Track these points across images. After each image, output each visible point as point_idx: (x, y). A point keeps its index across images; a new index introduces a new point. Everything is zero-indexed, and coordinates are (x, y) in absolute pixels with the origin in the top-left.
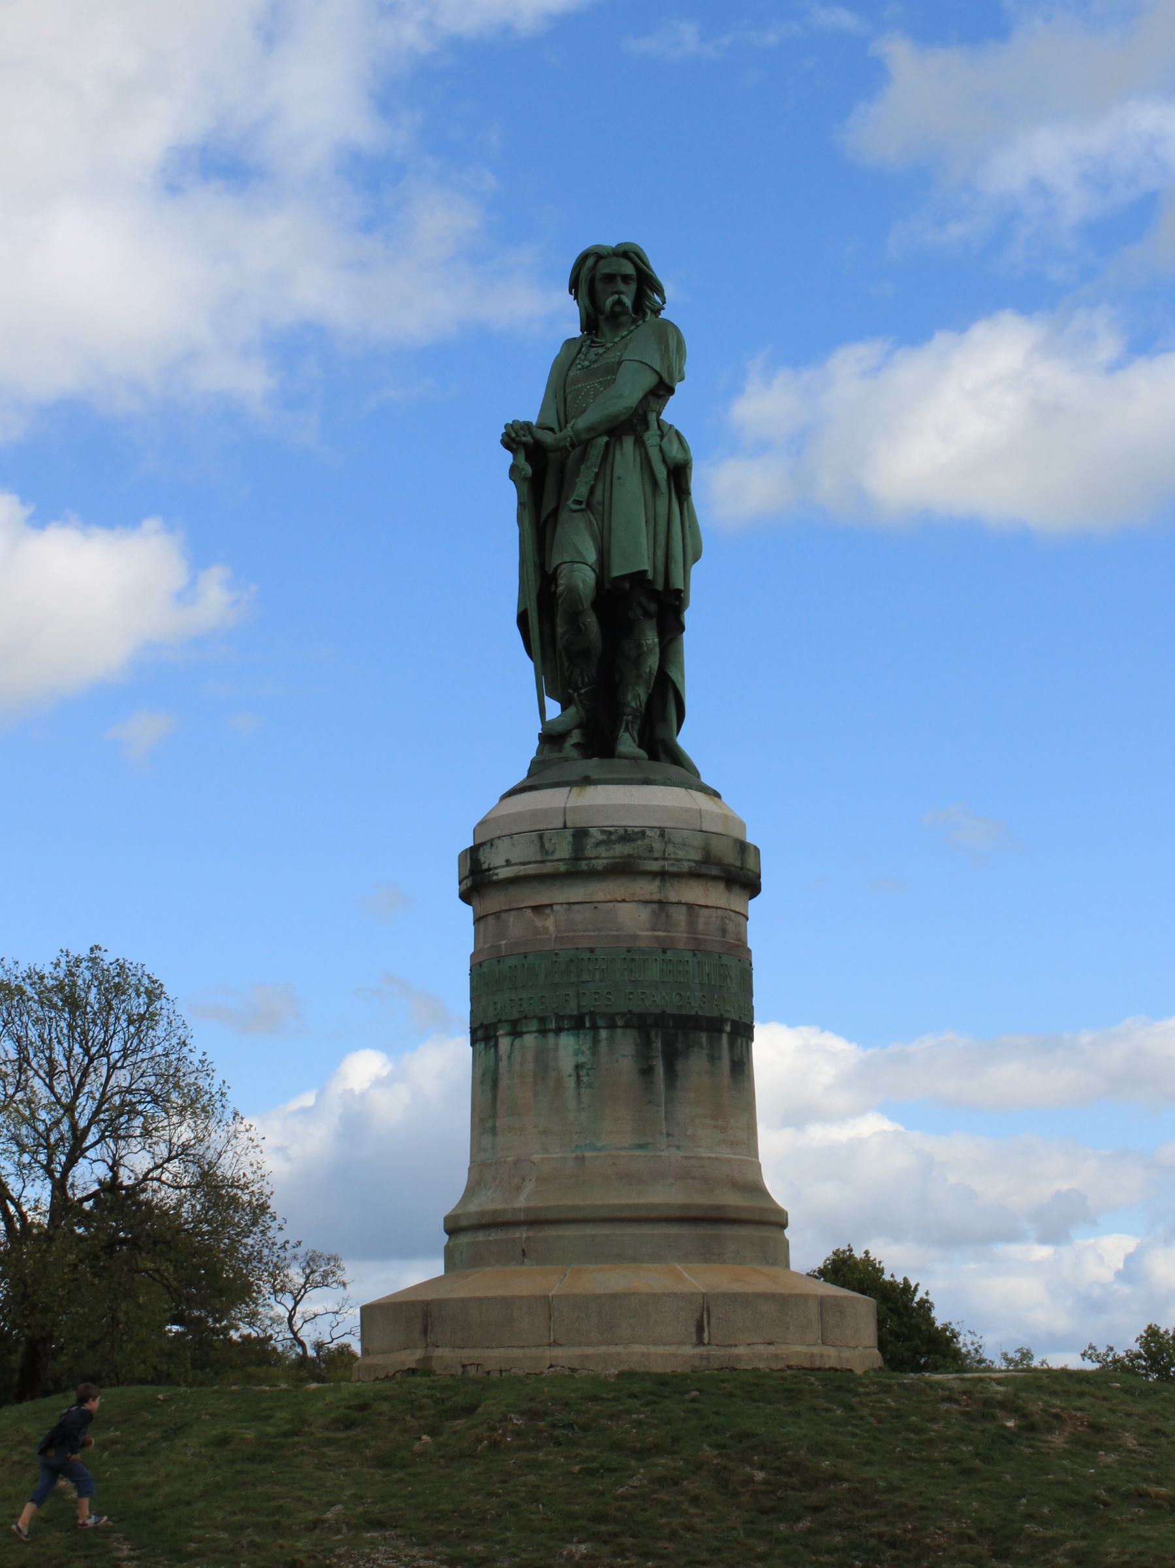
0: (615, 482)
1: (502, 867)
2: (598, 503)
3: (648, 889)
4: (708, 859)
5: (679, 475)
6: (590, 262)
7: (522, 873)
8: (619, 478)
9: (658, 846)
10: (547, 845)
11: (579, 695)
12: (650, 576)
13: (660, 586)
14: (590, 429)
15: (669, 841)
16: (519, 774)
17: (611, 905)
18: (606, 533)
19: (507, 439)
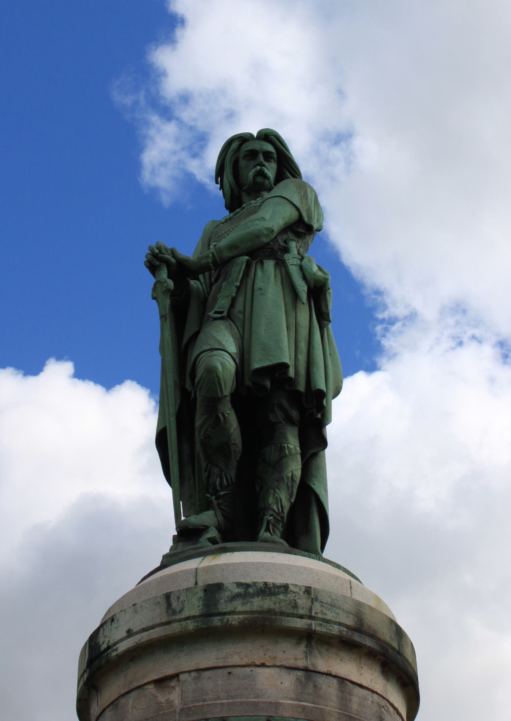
0: (256, 293)
2: (239, 312)
3: (293, 653)
4: (359, 628)
5: (318, 292)
7: (144, 640)
8: (260, 289)
9: (303, 602)
10: (175, 604)
11: (217, 498)
13: (302, 387)
14: (232, 247)
15: (317, 599)
17: (248, 670)
18: (246, 336)
19: (150, 257)
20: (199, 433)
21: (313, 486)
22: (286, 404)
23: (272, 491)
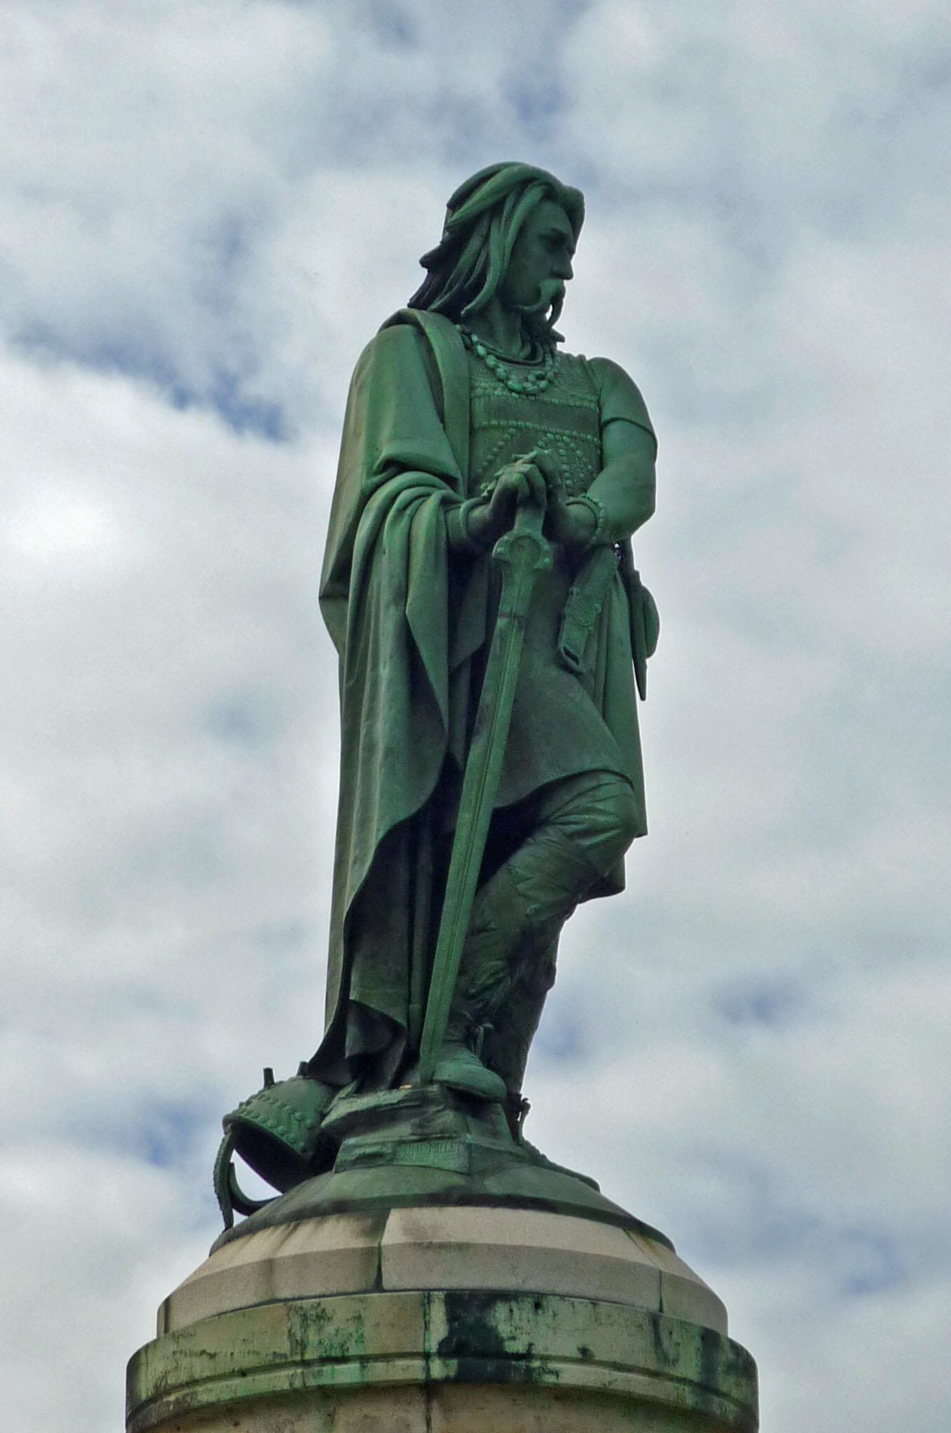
1: (565, 1359)
6: (532, 196)
20: (537, 912)
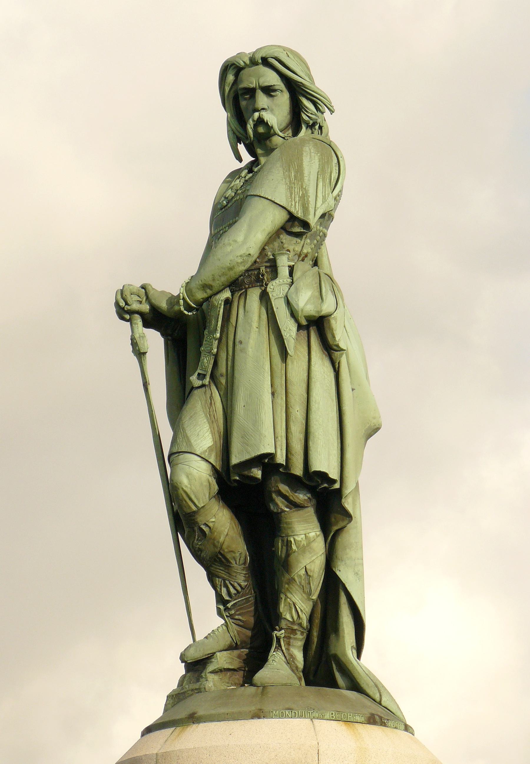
12: (281, 459)
13: (298, 470)
16: (155, 711)
21: (338, 573)
22: (284, 488)
23: (282, 596)
